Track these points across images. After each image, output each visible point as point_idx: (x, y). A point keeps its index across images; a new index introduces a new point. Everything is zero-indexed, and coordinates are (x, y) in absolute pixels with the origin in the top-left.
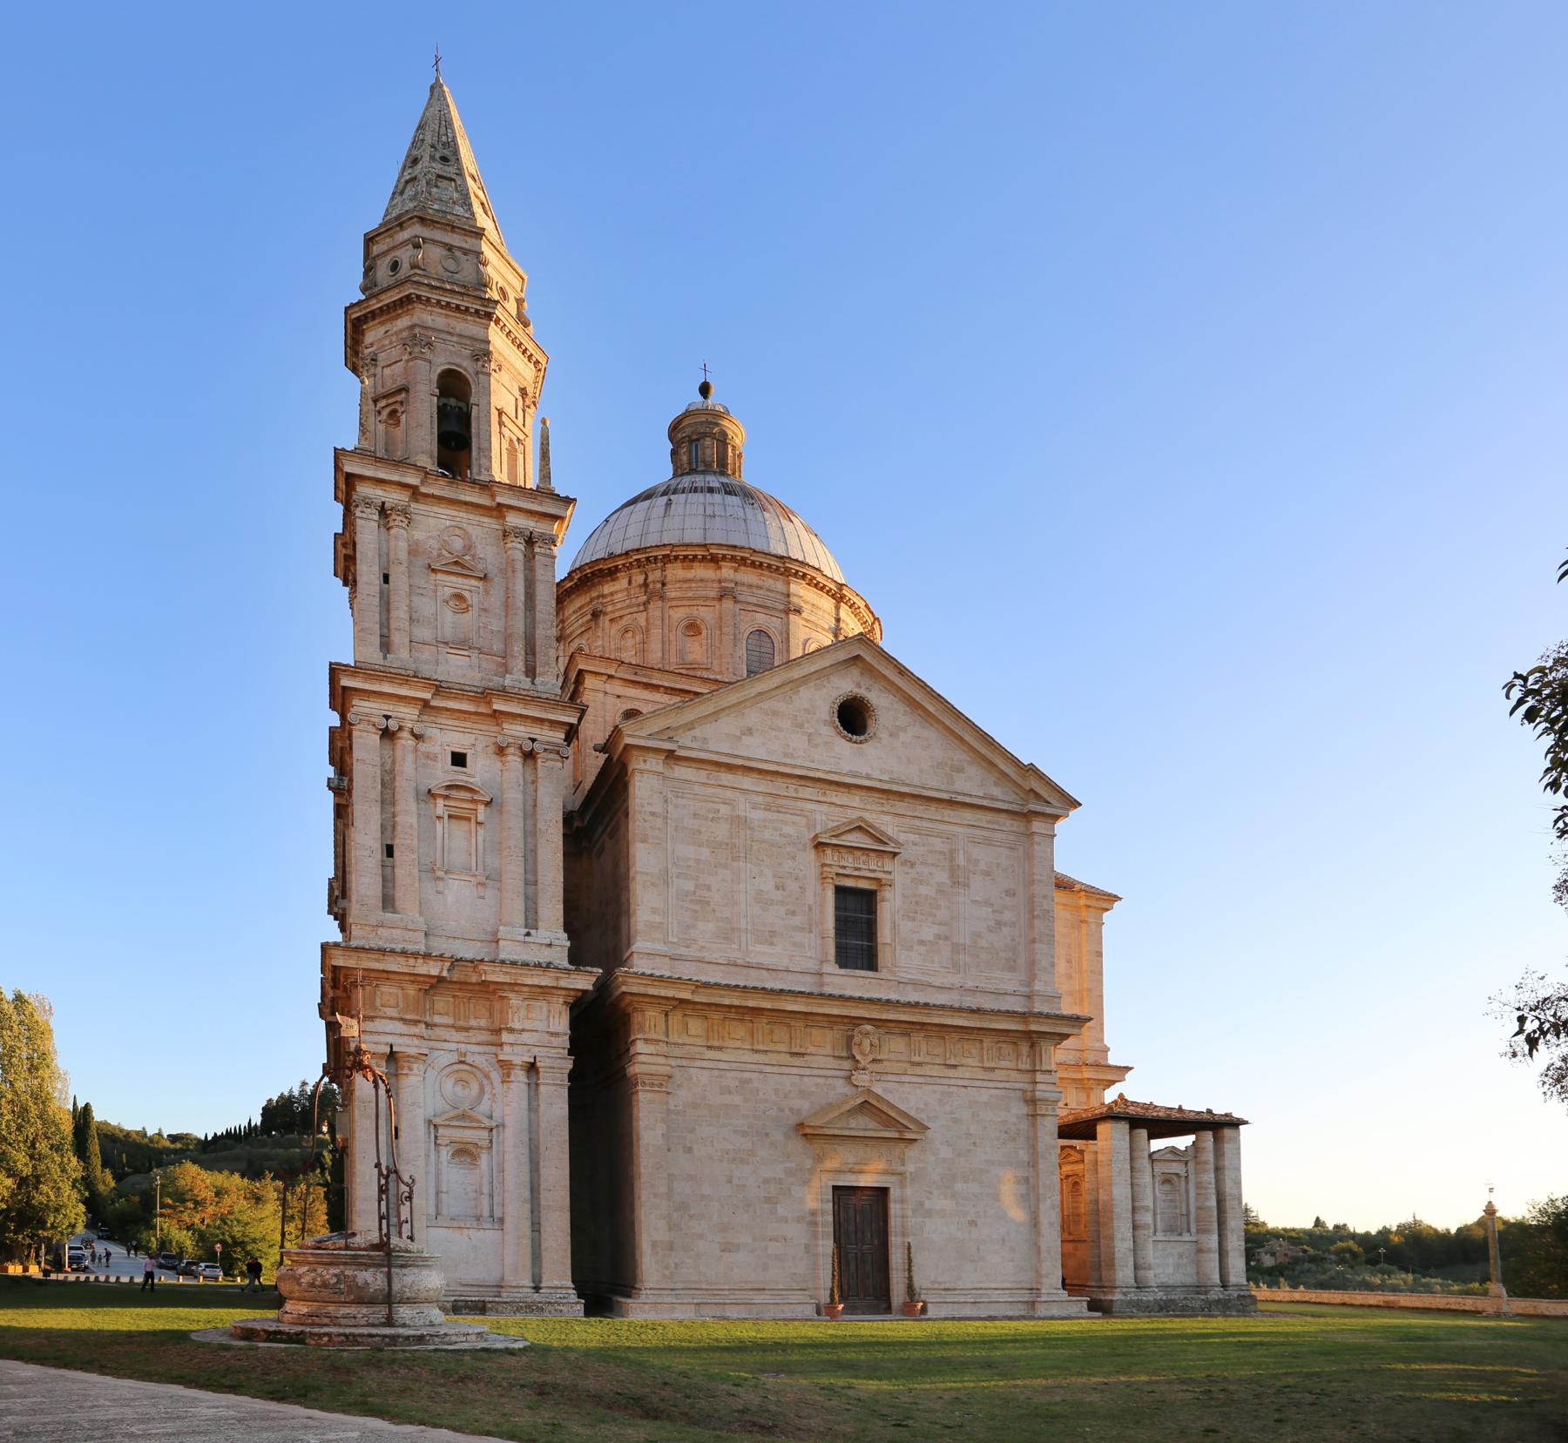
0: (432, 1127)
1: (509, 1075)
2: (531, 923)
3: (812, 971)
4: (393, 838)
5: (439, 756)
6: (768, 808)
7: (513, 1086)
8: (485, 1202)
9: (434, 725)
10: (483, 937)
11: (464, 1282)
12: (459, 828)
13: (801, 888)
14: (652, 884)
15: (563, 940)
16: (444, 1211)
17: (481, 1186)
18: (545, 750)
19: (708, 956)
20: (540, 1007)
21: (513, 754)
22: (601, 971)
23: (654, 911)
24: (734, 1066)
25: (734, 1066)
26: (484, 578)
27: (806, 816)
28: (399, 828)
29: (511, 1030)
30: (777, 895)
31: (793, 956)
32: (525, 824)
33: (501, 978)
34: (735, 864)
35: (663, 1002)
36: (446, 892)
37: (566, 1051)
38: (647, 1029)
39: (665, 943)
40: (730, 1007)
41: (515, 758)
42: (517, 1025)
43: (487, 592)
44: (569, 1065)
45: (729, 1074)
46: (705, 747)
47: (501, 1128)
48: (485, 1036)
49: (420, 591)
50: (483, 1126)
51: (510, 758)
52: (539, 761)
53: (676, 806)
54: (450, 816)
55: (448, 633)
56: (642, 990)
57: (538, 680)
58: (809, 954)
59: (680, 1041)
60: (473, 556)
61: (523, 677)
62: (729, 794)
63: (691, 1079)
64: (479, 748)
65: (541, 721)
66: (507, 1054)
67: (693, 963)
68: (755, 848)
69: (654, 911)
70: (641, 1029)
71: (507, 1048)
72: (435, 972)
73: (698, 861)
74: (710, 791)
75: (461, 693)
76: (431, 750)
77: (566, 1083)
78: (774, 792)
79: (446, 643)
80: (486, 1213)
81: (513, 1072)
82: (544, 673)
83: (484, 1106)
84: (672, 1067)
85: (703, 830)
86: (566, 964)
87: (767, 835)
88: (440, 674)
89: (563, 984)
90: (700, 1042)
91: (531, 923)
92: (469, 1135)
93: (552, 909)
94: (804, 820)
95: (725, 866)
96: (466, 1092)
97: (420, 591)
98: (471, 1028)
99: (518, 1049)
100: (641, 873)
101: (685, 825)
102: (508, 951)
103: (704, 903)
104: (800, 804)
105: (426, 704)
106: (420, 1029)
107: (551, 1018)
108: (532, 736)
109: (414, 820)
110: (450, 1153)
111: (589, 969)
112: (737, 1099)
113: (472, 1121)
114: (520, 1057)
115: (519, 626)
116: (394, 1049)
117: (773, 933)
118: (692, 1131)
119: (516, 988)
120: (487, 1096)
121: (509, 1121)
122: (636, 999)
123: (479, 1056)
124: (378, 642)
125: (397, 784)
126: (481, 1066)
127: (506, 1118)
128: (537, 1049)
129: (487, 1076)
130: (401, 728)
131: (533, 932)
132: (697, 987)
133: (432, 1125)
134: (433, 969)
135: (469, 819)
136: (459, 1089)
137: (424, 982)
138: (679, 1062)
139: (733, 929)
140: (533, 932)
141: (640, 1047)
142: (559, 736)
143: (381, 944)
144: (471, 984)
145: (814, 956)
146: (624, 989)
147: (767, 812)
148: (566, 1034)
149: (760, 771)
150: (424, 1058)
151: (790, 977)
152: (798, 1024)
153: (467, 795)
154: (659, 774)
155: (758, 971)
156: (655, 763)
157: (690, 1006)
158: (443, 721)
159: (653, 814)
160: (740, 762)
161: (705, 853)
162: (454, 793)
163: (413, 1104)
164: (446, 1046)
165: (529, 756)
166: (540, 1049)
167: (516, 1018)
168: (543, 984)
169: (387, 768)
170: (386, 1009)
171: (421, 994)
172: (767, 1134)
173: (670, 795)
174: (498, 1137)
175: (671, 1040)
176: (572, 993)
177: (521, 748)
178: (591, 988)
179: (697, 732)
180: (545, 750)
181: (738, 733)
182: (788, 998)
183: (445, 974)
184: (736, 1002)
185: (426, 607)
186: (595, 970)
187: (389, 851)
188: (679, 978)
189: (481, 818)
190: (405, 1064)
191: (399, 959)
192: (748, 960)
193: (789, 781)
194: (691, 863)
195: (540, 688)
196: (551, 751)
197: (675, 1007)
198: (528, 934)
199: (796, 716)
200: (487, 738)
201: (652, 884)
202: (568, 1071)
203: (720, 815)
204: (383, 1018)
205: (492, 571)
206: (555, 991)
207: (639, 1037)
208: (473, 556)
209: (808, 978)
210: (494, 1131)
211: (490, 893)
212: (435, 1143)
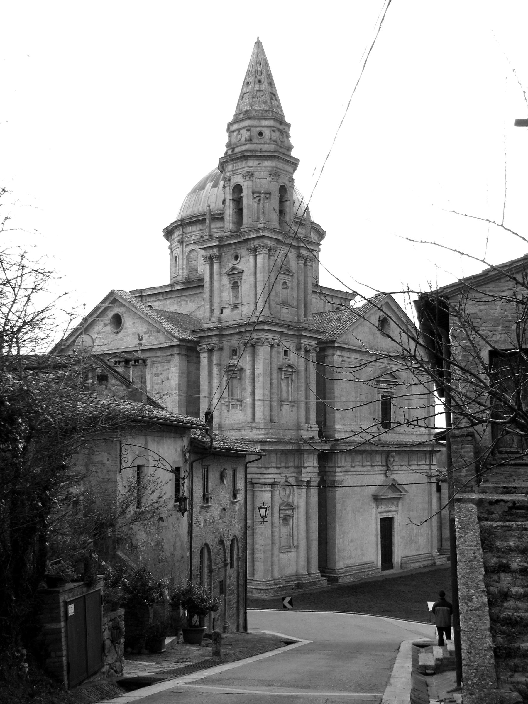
10: (294, 428)
20: (311, 457)
42: (306, 466)
99: (305, 475)
128: (310, 474)
211: (294, 409)
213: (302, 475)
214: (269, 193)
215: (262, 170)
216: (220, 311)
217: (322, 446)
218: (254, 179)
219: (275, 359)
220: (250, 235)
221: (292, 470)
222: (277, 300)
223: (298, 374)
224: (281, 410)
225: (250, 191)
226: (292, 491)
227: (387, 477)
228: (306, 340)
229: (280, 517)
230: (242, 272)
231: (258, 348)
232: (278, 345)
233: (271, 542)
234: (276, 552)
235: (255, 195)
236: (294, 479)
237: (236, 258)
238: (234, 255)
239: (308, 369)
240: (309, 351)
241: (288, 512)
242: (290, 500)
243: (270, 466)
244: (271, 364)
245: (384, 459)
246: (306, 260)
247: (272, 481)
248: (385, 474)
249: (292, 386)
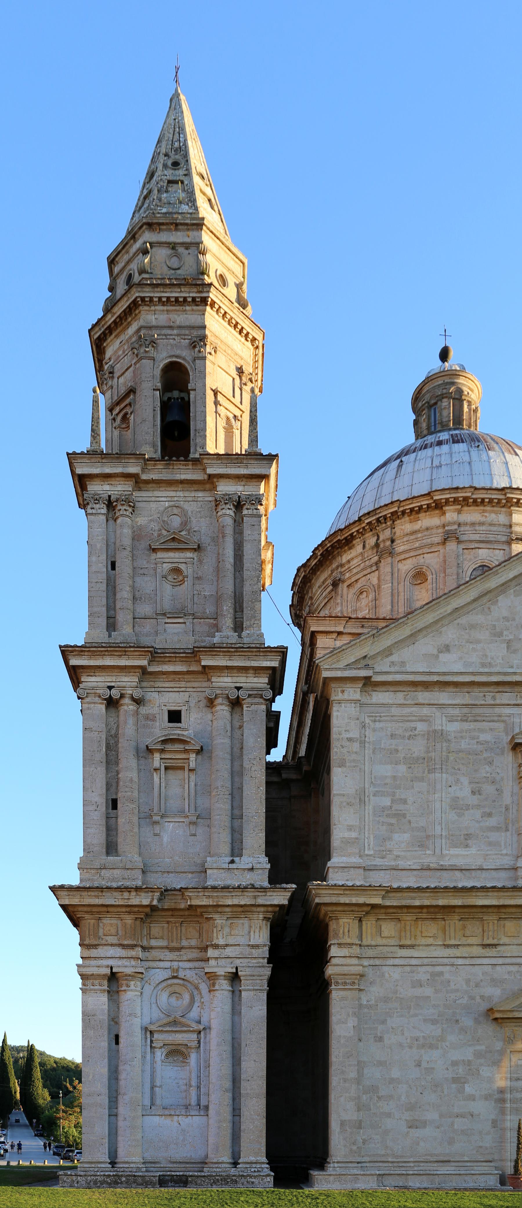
0: (148, 1033)
1: (214, 985)
2: (236, 850)
3: (506, 867)
4: (116, 794)
5: (157, 716)
6: (464, 719)
7: (217, 994)
8: (193, 1092)
9: (153, 690)
10: (194, 869)
11: (173, 1160)
12: (174, 777)
13: (497, 790)
14: (348, 804)
15: (264, 863)
16: (158, 1102)
17: (190, 1080)
18: (250, 696)
19: (401, 864)
21: (222, 704)
22: (294, 886)
23: (350, 828)
24: (426, 961)
25: (426, 961)
26: (198, 549)
27: (503, 721)
28: (121, 783)
29: (216, 946)
30: (474, 800)
31: (487, 855)
32: (232, 766)
33: (205, 902)
34: (432, 776)
35: (356, 909)
36: (162, 834)
37: (266, 960)
38: (341, 935)
39: (360, 856)
40: (421, 907)
41: (223, 707)
42: (221, 942)
43: (200, 561)
44: (267, 972)
45: (424, 969)
46: (403, 669)
47: (208, 1030)
48: (195, 954)
49: (142, 572)
50: (191, 1029)
51: (218, 708)
52: (245, 706)
53: (374, 730)
54: (166, 768)
55: (167, 606)
56: (334, 900)
57: (244, 634)
58: (504, 852)
59: (373, 943)
60: (189, 531)
61: (231, 633)
62: (425, 711)
63: (383, 975)
64: (192, 704)
65: (244, 669)
66: (212, 966)
67: (388, 872)
68: (452, 758)
69: (350, 828)
70: (336, 935)
71: (212, 962)
72: (146, 902)
73: (394, 778)
74: (407, 711)
75: (174, 655)
76: (151, 711)
77: (266, 987)
78: (473, 702)
79: (164, 614)
80: (194, 1102)
81: (217, 982)
82: (250, 626)
83: (194, 1014)
84: (364, 967)
85: (400, 748)
86: (266, 884)
87: (464, 745)
88: (159, 643)
89: (260, 901)
90: (392, 942)
91: (236, 850)
92: (180, 1038)
94: (501, 726)
95: (422, 779)
96: (180, 1002)
97: (142, 572)
99: (222, 962)
100: (338, 795)
101: (382, 746)
102: (215, 878)
104: (497, 710)
105: (143, 671)
106: (138, 952)
107: (252, 933)
108: (238, 685)
109: (134, 775)
110: (164, 1054)
111: (284, 885)
112: (428, 991)
113: (183, 1026)
114: (223, 968)
115: (228, 586)
116: (114, 970)
117: (468, 836)
118: (384, 1022)
119: (219, 910)
120: (197, 1004)
121: (214, 1024)
122: (330, 908)
123: (187, 970)
124: (104, 623)
125: (120, 745)
126: (191, 980)
127: (212, 1021)
129: (197, 988)
130: (122, 696)
131: (237, 859)
132: (387, 892)
133: (149, 1032)
134: (145, 900)
135: (182, 768)
136: (173, 1000)
137: (139, 912)
138: (372, 962)
139: (428, 837)
140: (237, 859)
141: (334, 951)
142: (263, 681)
143: (104, 883)
144: (180, 910)
145: (509, 852)
146: (317, 900)
147: (465, 723)
148: (265, 945)
149: (456, 684)
150: (140, 976)
151: (484, 874)
152: (491, 918)
153: (180, 747)
154: (356, 701)
155: (451, 873)
156: (353, 692)
157: (383, 911)
158: (161, 685)
159: (350, 740)
160: (435, 678)
161: (402, 769)
162: (169, 747)
163: (130, 1015)
164: (162, 964)
165: (236, 704)
166: (241, 960)
167: (220, 937)
168: (242, 903)
169: (113, 732)
170: (107, 938)
171: (138, 922)
172: (457, 1021)
173: (367, 721)
174: (205, 1038)
175: (365, 942)
176: (270, 909)
177: (228, 698)
178: (286, 902)
179: (394, 658)
180: (250, 696)
181: (435, 652)
182: (479, 894)
183: (155, 903)
184: (427, 902)
185: (147, 584)
186: (289, 886)
187: (114, 804)
188: (370, 886)
189: (192, 765)
190: (124, 982)
191: (115, 894)
192: (442, 863)
193: (486, 689)
194: (388, 781)
195: (246, 640)
196: (255, 696)
197: (367, 913)
198: (232, 862)
199: (494, 626)
200: (199, 694)
201: (348, 804)
202: (266, 977)
203: (416, 732)
204: (105, 945)
205: (205, 540)
206: (254, 909)
207: (332, 942)
208: (189, 531)
209: (503, 874)
210: (202, 1033)
211: (200, 830)
212: (151, 1047)
246: (239, 506)
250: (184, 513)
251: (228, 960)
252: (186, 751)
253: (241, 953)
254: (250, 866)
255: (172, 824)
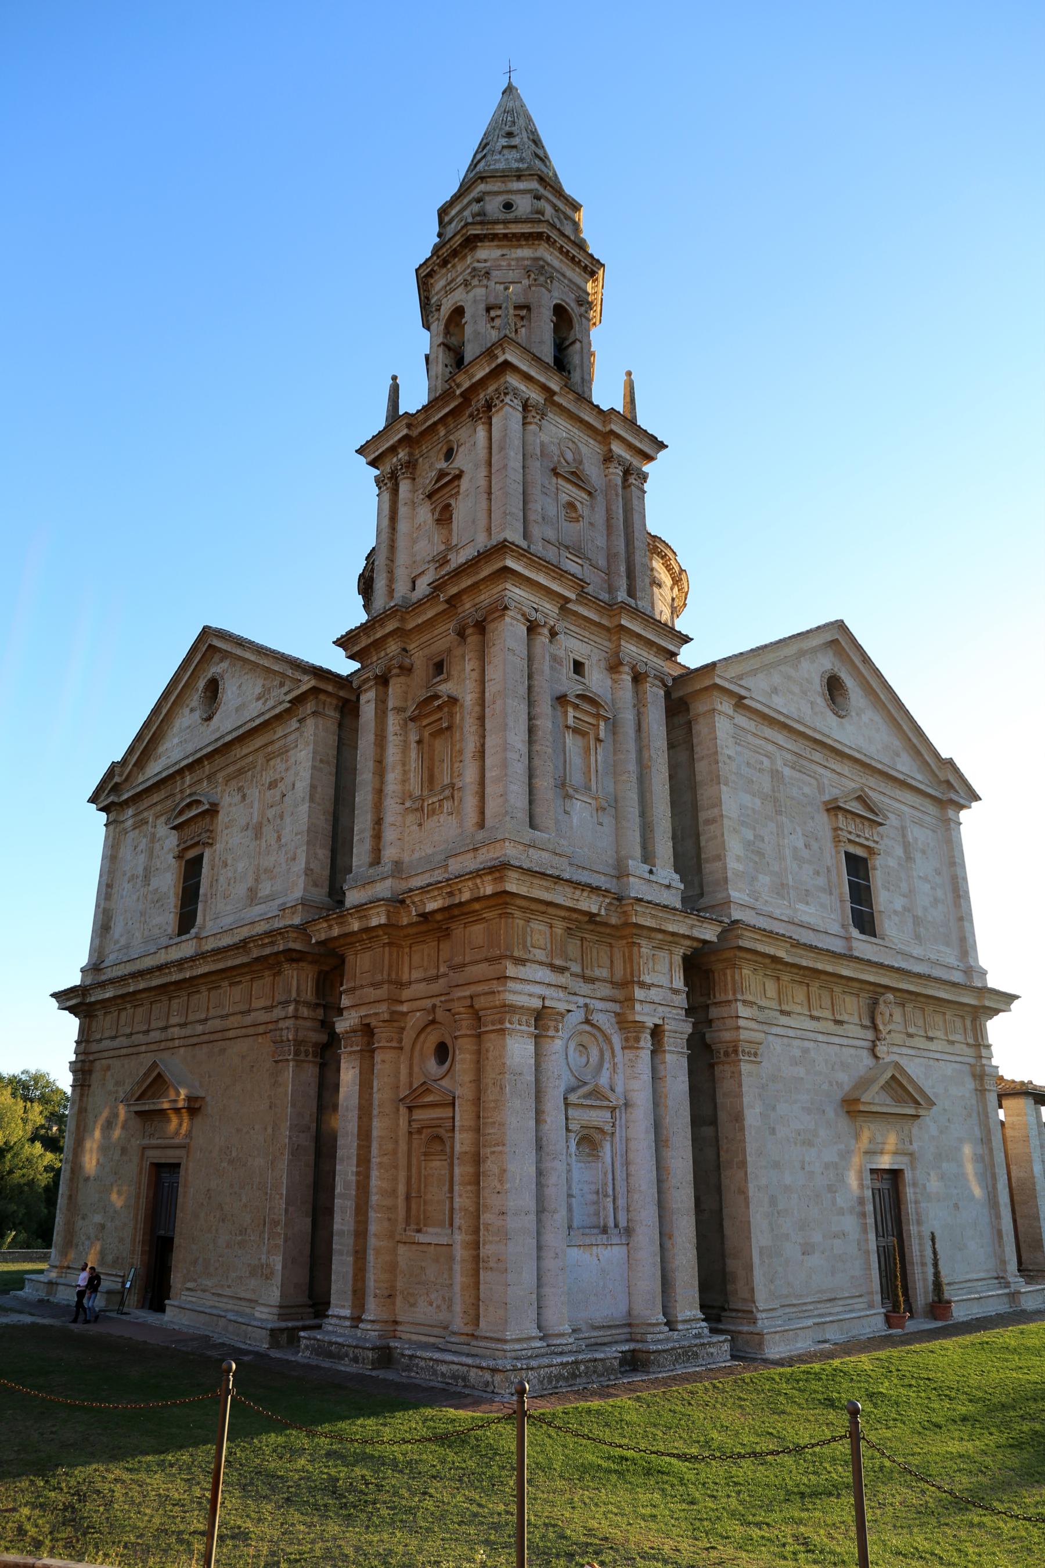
21: (628, 674)
26: (590, 494)
29: (642, 985)
42: (647, 979)
65: (650, 644)
93: (664, 848)
98: (597, 979)
99: (648, 1008)
103: (761, 854)
128: (660, 1009)
140: (654, 869)
165: (637, 678)
213: (638, 1007)
214: (528, 308)
215: (509, 265)
216: (410, 585)
217: (692, 926)
218: (492, 284)
219: (544, 665)
220: (473, 376)
221: (605, 990)
222: (550, 534)
223: (614, 726)
224: (566, 812)
225: (482, 306)
226: (607, 1055)
227: (876, 1057)
228: (634, 648)
229: (568, 1130)
230: (459, 477)
231: (490, 627)
232: (553, 634)
233: (532, 1205)
234: (554, 1238)
235: (493, 313)
236: (614, 1020)
237: (449, 455)
238: (445, 450)
239: (644, 726)
240: (646, 675)
241: (599, 1117)
242: (604, 1080)
243: (531, 957)
244: (530, 677)
245: (865, 1010)
247: (537, 1003)
248: (873, 1051)
249: (600, 756)
250: (580, 454)
251: (653, 1006)
252: (598, 716)
253: (664, 999)
254: (666, 882)
255: (579, 803)
